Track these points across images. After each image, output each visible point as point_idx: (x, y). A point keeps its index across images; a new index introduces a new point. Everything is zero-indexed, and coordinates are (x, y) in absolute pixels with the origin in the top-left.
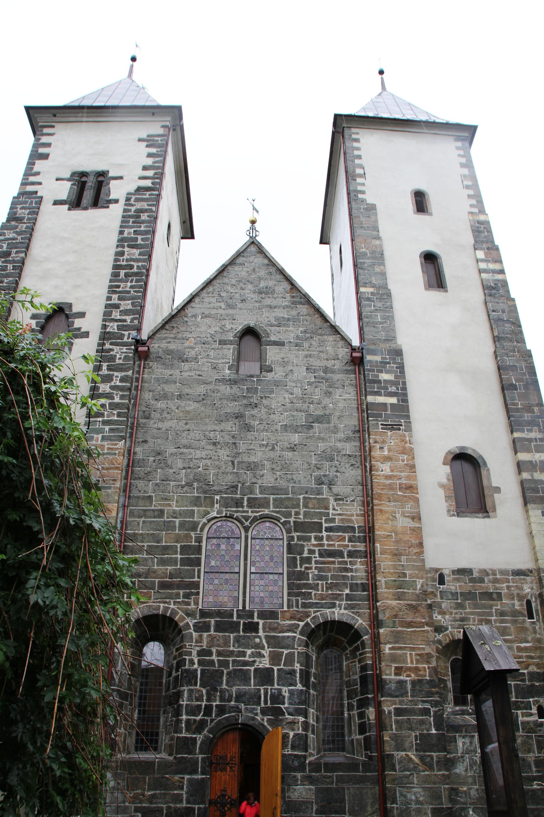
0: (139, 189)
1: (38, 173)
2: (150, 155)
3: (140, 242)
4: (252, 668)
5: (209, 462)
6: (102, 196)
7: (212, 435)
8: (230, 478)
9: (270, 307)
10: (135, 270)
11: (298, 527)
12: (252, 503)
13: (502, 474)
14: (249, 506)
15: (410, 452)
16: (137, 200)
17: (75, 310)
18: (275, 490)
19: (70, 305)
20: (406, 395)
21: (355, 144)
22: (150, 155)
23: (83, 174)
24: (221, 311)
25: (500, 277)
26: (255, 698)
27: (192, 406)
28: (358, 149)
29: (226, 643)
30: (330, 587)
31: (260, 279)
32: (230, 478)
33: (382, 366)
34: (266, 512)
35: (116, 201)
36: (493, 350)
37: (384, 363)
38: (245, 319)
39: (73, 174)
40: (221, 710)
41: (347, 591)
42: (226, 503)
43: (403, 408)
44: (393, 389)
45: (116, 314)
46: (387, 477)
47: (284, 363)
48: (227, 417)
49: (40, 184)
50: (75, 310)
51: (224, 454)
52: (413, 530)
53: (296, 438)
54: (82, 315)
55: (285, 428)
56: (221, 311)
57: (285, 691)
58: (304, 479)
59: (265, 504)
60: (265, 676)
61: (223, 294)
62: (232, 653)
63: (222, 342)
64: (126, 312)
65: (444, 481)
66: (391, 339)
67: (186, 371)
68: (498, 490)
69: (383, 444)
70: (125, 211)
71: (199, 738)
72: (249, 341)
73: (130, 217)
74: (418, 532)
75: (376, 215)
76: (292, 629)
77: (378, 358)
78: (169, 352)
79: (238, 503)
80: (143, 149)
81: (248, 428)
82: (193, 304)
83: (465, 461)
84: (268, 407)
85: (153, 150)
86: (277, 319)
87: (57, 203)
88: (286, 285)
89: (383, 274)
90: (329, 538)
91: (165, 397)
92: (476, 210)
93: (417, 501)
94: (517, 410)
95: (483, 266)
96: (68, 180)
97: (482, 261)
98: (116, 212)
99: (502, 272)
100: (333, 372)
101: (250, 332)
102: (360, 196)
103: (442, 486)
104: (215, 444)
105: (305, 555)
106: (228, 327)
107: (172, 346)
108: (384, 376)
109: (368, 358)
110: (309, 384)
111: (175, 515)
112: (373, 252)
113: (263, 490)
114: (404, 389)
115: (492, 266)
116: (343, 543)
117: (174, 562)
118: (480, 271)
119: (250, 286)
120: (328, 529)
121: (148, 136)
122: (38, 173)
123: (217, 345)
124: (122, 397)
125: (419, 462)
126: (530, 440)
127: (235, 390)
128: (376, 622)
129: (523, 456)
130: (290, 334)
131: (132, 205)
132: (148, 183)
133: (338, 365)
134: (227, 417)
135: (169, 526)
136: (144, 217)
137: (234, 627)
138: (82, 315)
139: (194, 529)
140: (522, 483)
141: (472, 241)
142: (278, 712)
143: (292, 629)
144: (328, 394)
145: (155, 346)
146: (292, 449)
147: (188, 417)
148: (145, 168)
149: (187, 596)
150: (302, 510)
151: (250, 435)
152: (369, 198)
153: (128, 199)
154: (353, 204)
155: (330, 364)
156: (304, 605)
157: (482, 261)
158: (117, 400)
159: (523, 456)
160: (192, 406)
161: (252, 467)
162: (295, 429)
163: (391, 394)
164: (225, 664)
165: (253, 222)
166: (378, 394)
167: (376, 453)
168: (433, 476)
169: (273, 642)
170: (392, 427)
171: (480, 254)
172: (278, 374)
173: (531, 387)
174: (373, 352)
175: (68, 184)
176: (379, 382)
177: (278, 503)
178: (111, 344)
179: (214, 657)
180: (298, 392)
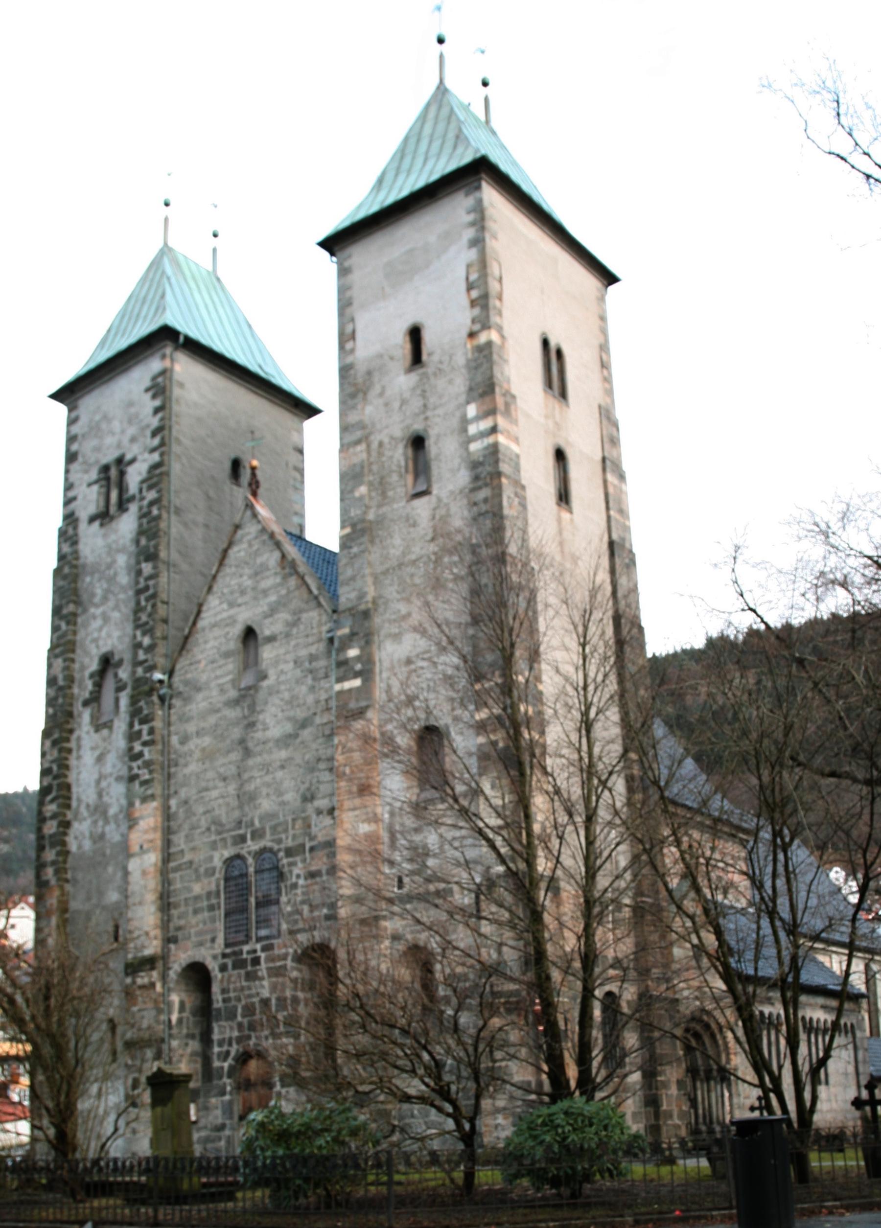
4: (256, 1000)
5: (221, 801)
7: (222, 770)
11: (289, 852)
14: (253, 839)
18: (272, 816)
19: (112, 653)
23: (106, 469)
24: (225, 615)
25: (491, 440)
32: (236, 814)
38: (245, 616)
41: (325, 911)
44: (358, 667)
47: (276, 662)
51: (232, 789)
53: (283, 754)
61: (226, 591)
63: (227, 655)
70: (141, 508)
71: (226, 1065)
79: (242, 839)
82: (203, 615)
87: (92, 520)
95: (472, 429)
96: (96, 482)
101: (249, 634)
104: (225, 779)
105: (294, 880)
120: (312, 849)
121: (154, 378)
123: (222, 662)
132: (156, 457)
146: (282, 767)
147: (208, 756)
150: (291, 832)
151: (251, 762)
153: (141, 491)
155: (313, 650)
160: (207, 741)
163: (357, 675)
171: (472, 410)
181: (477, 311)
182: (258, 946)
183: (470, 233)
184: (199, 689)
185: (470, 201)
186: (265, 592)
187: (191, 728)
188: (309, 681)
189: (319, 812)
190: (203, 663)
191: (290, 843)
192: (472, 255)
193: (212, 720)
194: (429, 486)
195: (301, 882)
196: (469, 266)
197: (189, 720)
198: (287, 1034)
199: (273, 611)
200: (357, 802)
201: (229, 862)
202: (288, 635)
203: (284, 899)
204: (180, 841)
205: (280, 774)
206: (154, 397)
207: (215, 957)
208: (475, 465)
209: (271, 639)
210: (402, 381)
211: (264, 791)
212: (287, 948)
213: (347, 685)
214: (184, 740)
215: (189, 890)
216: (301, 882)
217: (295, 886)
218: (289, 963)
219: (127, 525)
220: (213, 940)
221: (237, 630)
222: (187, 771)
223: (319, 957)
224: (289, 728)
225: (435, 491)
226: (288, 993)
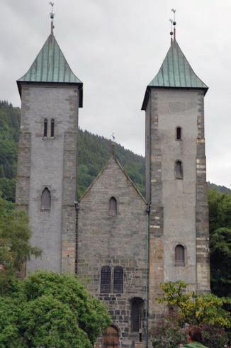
11: (128, 269)
27: (95, 228)
30: (136, 287)
32: (107, 253)
35: (61, 136)
44: (159, 223)
47: (124, 211)
49: (29, 125)
51: (106, 245)
52: (161, 271)
53: (127, 240)
57: (123, 316)
59: (117, 262)
63: (104, 203)
66: (160, 202)
67: (91, 215)
69: (156, 242)
72: (113, 202)
78: (86, 207)
81: (112, 236)
83: (180, 247)
87: (38, 136)
92: (200, 137)
95: (198, 166)
96: (40, 123)
97: (198, 164)
98: (61, 140)
99: (205, 169)
100: (140, 214)
108: (157, 218)
115: (201, 167)
116: (140, 274)
118: (197, 169)
119: (112, 179)
127: (108, 222)
128: (148, 298)
129: (198, 246)
130: (126, 199)
133: (142, 212)
135: (90, 270)
137: (109, 299)
138: (55, 190)
140: (197, 255)
144: (138, 223)
146: (126, 243)
151: (113, 239)
155: (139, 211)
157: (198, 164)
159: (198, 246)
160: (95, 228)
161: (114, 250)
163: (158, 225)
166: (153, 225)
167: (151, 246)
168: (169, 253)
171: (198, 161)
172: (122, 216)
177: (122, 261)
181: (200, 132)
182: (115, 294)
183: (199, 107)
184: (92, 211)
185: (199, 97)
186: (120, 188)
187: (88, 222)
188: (137, 221)
189: (139, 260)
190: (93, 203)
191: (128, 266)
192: (199, 114)
194: (182, 176)
196: (198, 117)
197: (87, 219)
198: (125, 322)
199: (123, 195)
200: (157, 260)
201: (103, 268)
203: (125, 282)
204: (81, 257)
205: (125, 245)
207: (97, 295)
208: (198, 177)
209: (122, 203)
210: (176, 143)
211: (119, 249)
212: (126, 296)
213: (155, 227)
214: (85, 225)
217: (130, 279)
218: (127, 301)
220: (96, 290)
221: (109, 197)
222: (86, 235)
223: (137, 303)
224: (129, 232)
225: (184, 180)
226: (126, 310)
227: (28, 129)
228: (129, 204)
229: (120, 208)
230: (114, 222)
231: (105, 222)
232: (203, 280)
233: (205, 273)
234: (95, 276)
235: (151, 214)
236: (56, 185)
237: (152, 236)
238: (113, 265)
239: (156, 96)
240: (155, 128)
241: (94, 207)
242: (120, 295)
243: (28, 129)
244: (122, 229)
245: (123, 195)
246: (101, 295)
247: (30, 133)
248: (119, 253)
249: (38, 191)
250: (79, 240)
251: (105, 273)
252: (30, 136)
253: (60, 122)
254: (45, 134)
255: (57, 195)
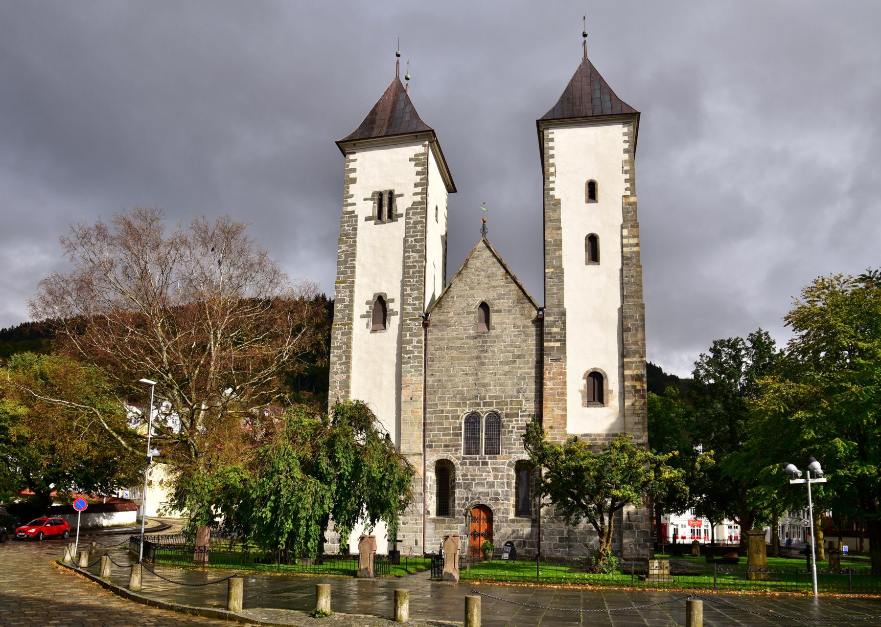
0: (414, 203)
1: (352, 196)
2: (418, 173)
3: (418, 248)
6: (394, 212)
8: (474, 392)
9: (494, 287)
10: (417, 269)
11: (507, 415)
12: (485, 404)
13: (613, 384)
15: (564, 374)
16: (414, 214)
17: (388, 297)
18: (496, 397)
20: (565, 340)
21: (551, 144)
22: (418, 173)
23: (381, 194)
24: (467, 292)
25: (635, 249)
26: (487, 494)
27: (455, 353)
28: (552, 148)
29: (474, 470)
31: (488, 267)
32: (474, 393)
33: (553, 324)
34: (491, 408)
35: (401, 215)
36: (619, 306)
37: (555, 321)
39: (373, 194)
40: (473, 499)
42: (472, 405)
43: (563, 349)
44: (558, 337)
45: (410, 301)
46: (551, 389)
47: (502, 323)
48: (472, 358)
49: (354, 204)
50: (388, 297)
51: (471, 379)
52: (562, 416)
53: (507, 368)
54: (392, 300)
55: (502, 363)
56: (467, 292)
58: (511, 390)
59: (491, 404)
60: (492, 485)
62: (476, 475)
64: (415, 299)
65: (582, 388)
66: (561, 304)
67: (449, 333)
68: (611, 391)
70: (407, 223)
73: (410, 228)
74: (564, 417)
75: (560, 208)
76: (503, 464)
77: (552, 318)
78: (440, 321)
79: (478, 405)
80: (413, 169)
81: (483, 364)
84: (493, 352)
85: (419, 169)
86: (498, 295)
87: (367, 219)
88: (503, 271)
89: (560, 257)
90: (522, 420)
91: (439, 349)
92: (628, 193)
93: (566, 400)
94: (629, 344)
95: (625, 241)
96: (371, 199)
100: (528, 327)
101: (484, 306)
102: (551, 193)
103: (581, 391)
106: (471, 302)
107: (442, 318)
108: (555, 330)
109: (546, 318)
110: (515, 336)
111: (448, 412)
112: (555, 240)
113: (490, 397)
114: (565, 337)
117: (450, 435)
119: (482, 273)
121: (415, 155)
122: (352, 196)
124: (419, 352)
125: (568, 379)
126: (632, 363)
131: (411, 218)
132: (418, 198)
134: (472, 358)
135: (447, 418)
136: (419, 227)
138: (392, 300)
139: (458, 418)
141: (621, 222)
142: (497, 499)
143: (503, 464)
145: (432, 318)
146: (505, 374)
148: (416, 185)
149: (456, 450)
152: (557, 194)
153: (407, 214)
154: (546, 199)
156: (509, 453)
158: (416, 354)
160: (455, 353)
161: (484, 385)
162: (507, 363)
164: (474, 480)
165: (484, 222)
166: (550, 341)
167: (546, 376)
168: (576, 385)
169: (495, 470)
170: (557, 360)
173: (640, 329)
174: (549, 315)
175: (371, 203)
176: (551, 334)
177: (498, 403)
178: (410, 320)
179: (469, 477)
180: (508, 340)
181: (628, 185)
193: (459, 343)
195: (515, 430)
199: (501, 297)
202: (509, 311)
206: (415, 165)
213: (551, 344)
215: (442, 424)
216: (515, 430)
219: (397, 229)
227: (353, 212)
228: (509, 311)
229: (494, 318)
230: (485, 342)
231: (472, 342)
232: (636, 427)
233: (638, 415)
234: (454, 429)
235: (545, 324)
236: (393, 293)
237: (547, 360)
238: (484, 411)
239: (551, 136)
240: (551, 186)
241: (451, 322)
242: (495, 458)
243: (353, 212)
244: (498, 350)
245: (501, 297)
246: (464, 458)
247: (357, 216)
248: (493, 391)
249: (367, 303)
250: (429, 373)
251: (473, 420)
252: (356, 221)
253: (401, 195)
254: (379, 218)
255: (394, 306)
